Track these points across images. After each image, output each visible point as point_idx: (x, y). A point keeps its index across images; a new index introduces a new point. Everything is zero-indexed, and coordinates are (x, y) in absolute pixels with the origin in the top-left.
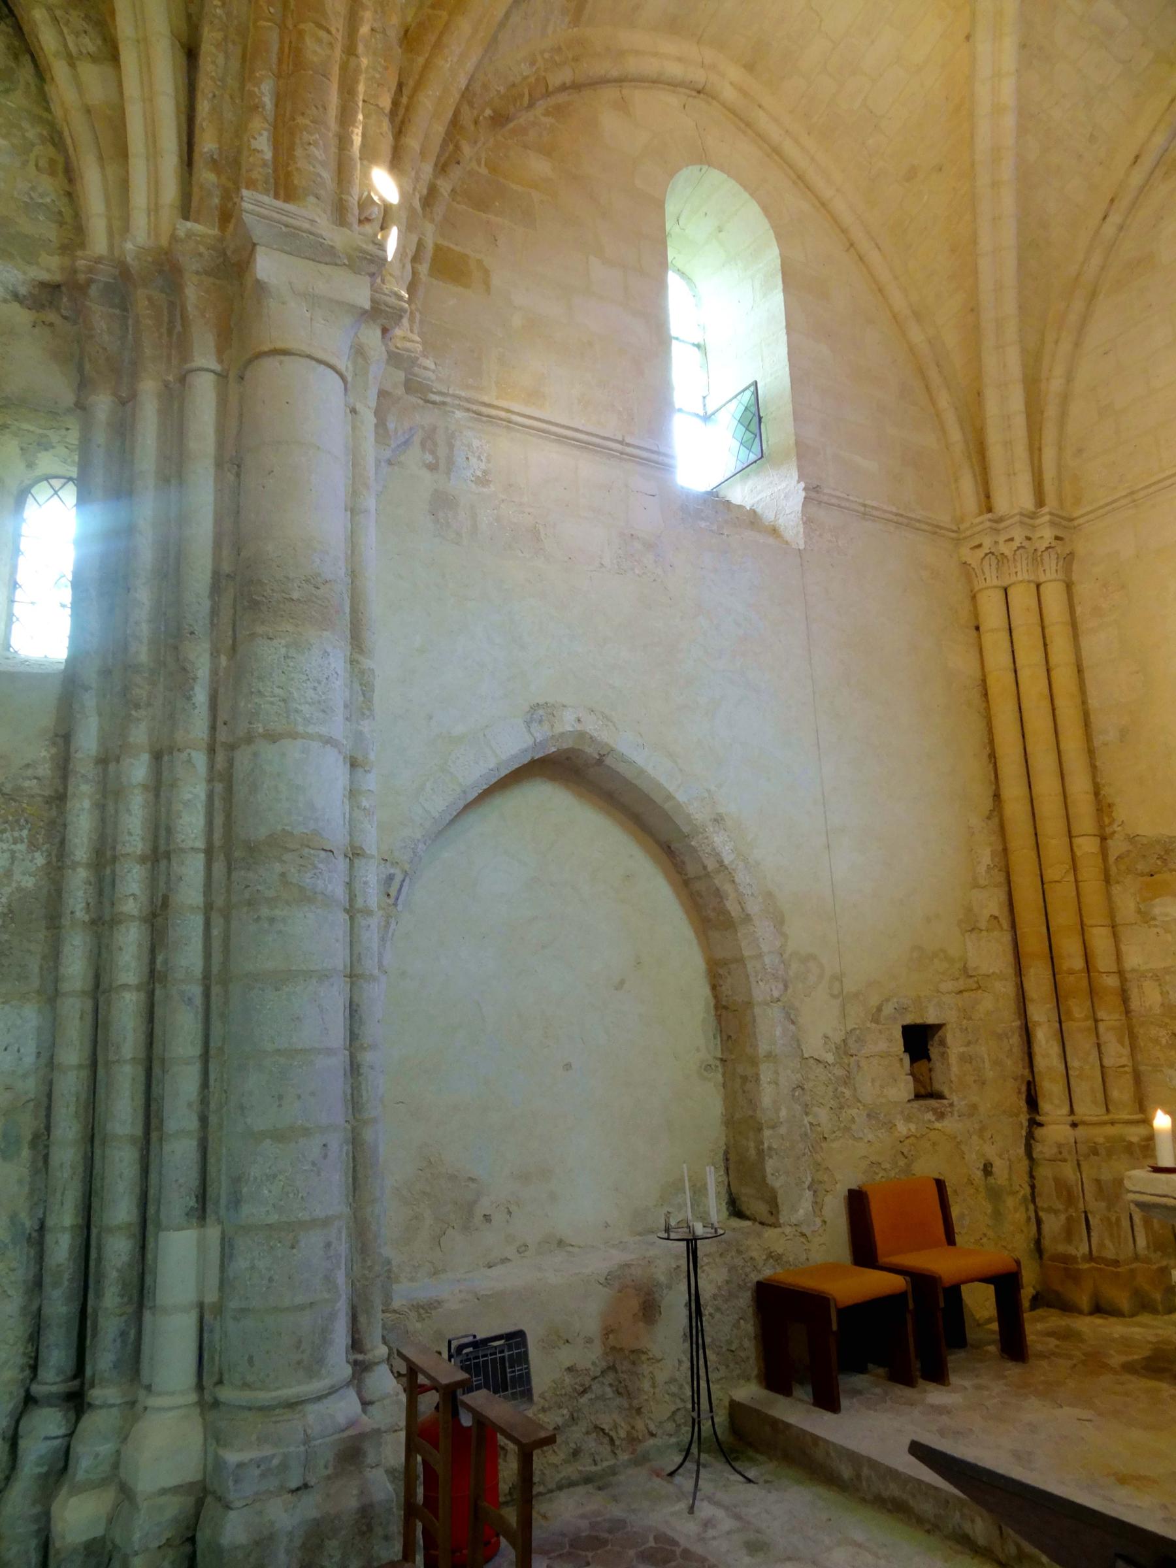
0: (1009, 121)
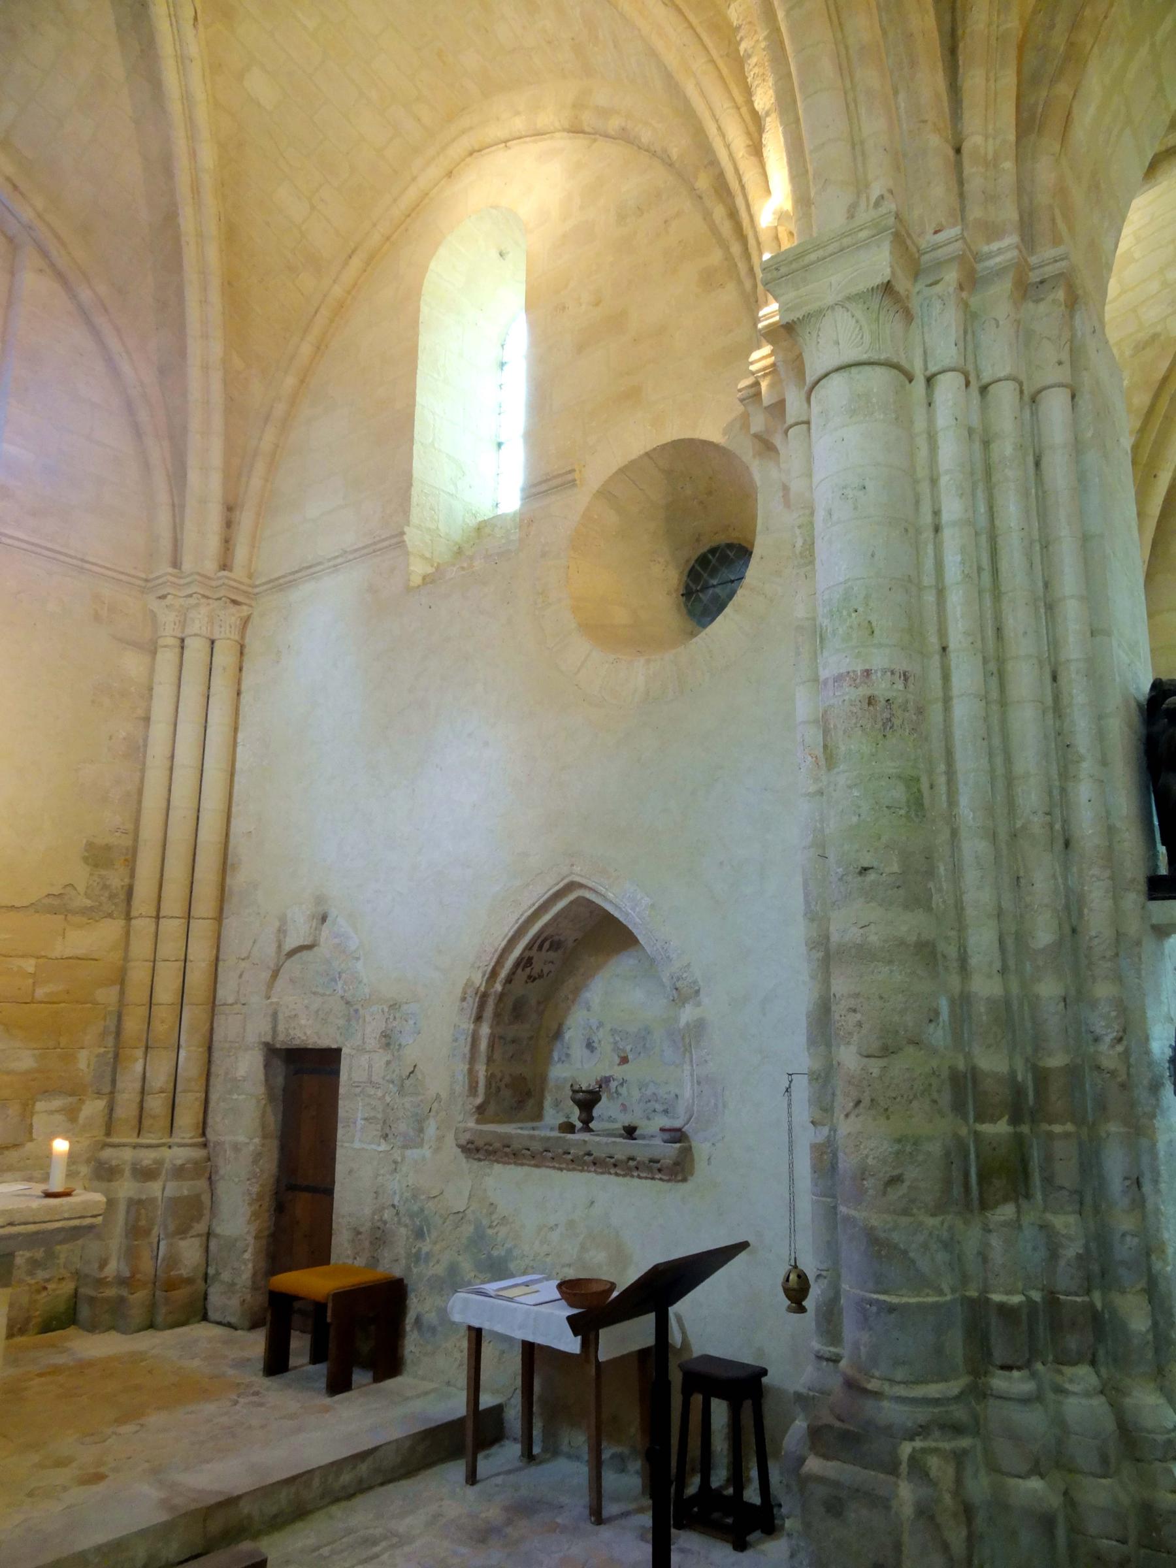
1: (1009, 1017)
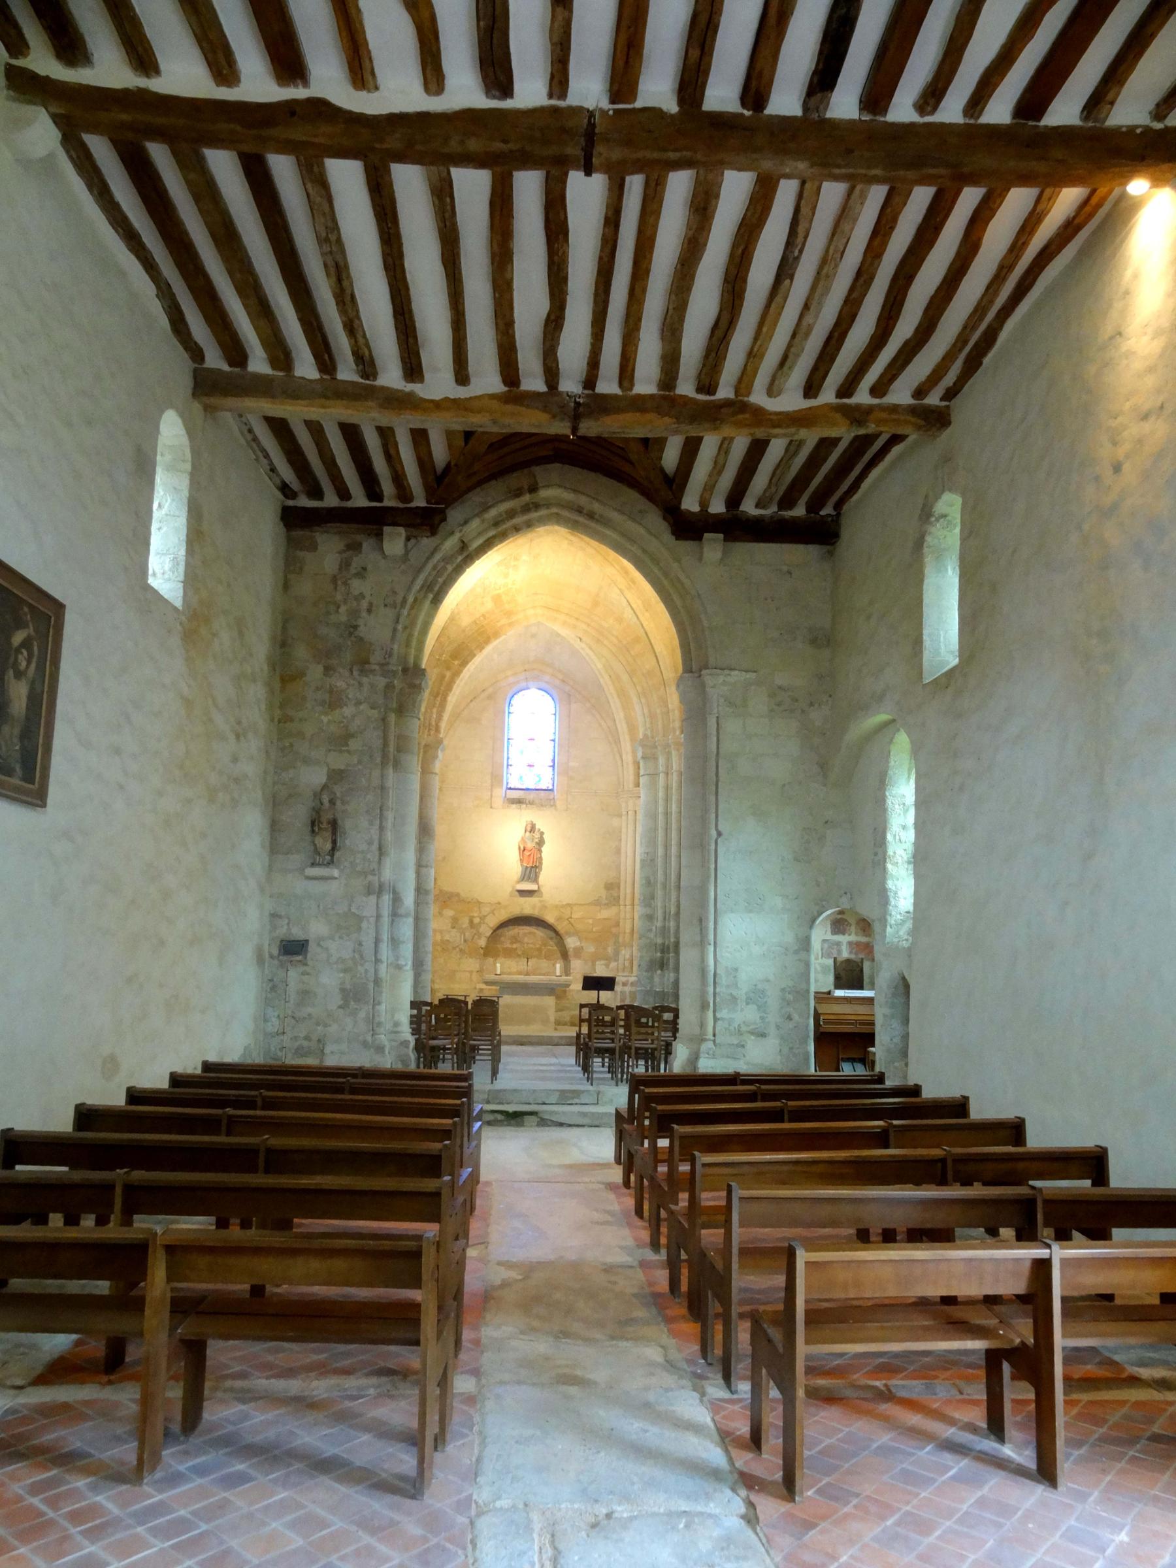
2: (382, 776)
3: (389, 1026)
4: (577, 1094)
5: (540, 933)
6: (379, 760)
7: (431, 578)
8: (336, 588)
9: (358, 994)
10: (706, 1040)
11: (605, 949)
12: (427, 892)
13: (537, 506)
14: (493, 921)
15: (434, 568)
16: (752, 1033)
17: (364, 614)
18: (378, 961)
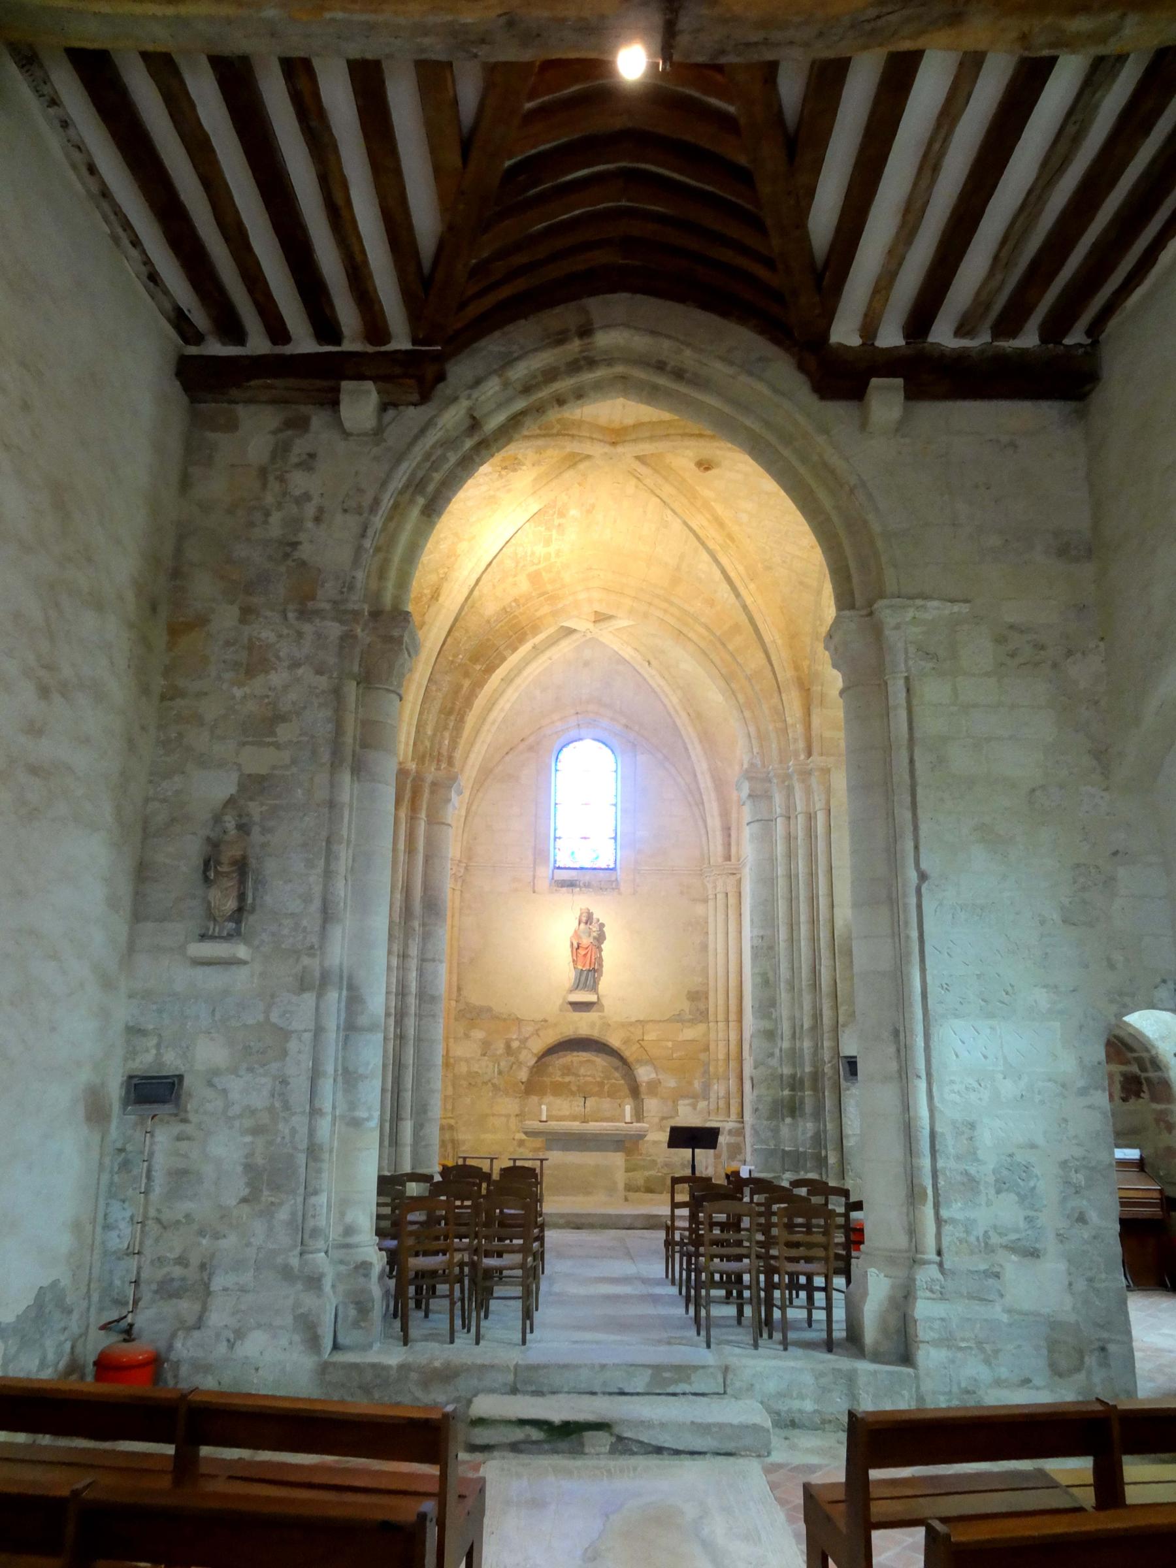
0: (503, 715)
1: (794, 1056)
2: (332, 785)
3: (334, 1234)
4: (683, 1371)
5: (601, 1061)
6: (325, 757)
7: (420, 474)
8: (264, 486)
9: (275, 1177)
10: (925, 1262)
11: (690, 1083)
12: (433, 999)
13: (591, 363)
14: (538, 1045)
15: (427, 456)
16: (1012, 1248)
17: (310, 525)
18: (315, 1112)
